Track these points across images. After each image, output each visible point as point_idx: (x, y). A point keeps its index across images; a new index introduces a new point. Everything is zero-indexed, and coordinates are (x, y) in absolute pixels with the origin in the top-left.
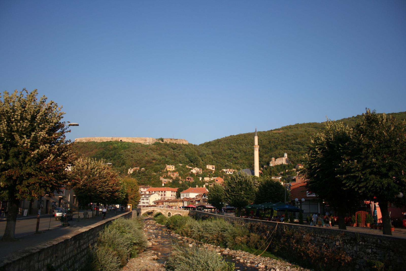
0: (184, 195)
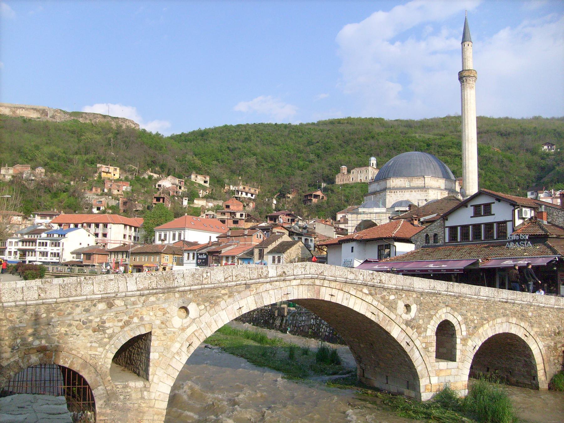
0: (165, 235)
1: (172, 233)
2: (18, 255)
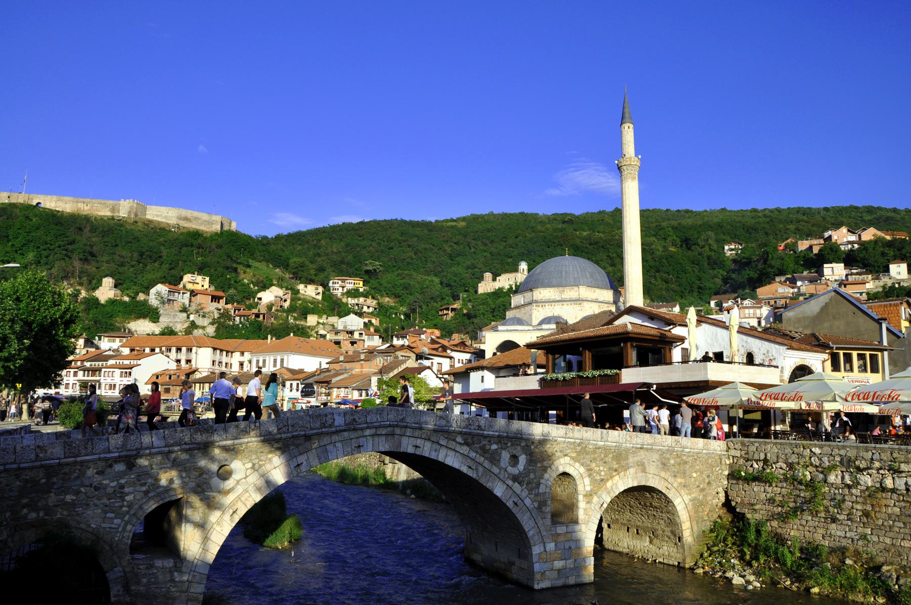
0: (264, 361)
1: (272, 358)
2: (78, 388)
